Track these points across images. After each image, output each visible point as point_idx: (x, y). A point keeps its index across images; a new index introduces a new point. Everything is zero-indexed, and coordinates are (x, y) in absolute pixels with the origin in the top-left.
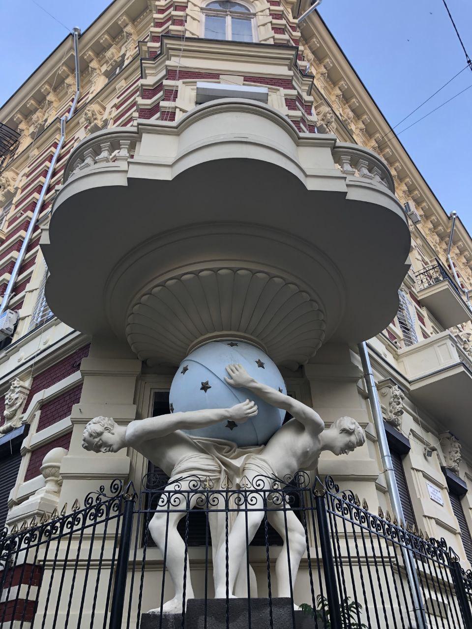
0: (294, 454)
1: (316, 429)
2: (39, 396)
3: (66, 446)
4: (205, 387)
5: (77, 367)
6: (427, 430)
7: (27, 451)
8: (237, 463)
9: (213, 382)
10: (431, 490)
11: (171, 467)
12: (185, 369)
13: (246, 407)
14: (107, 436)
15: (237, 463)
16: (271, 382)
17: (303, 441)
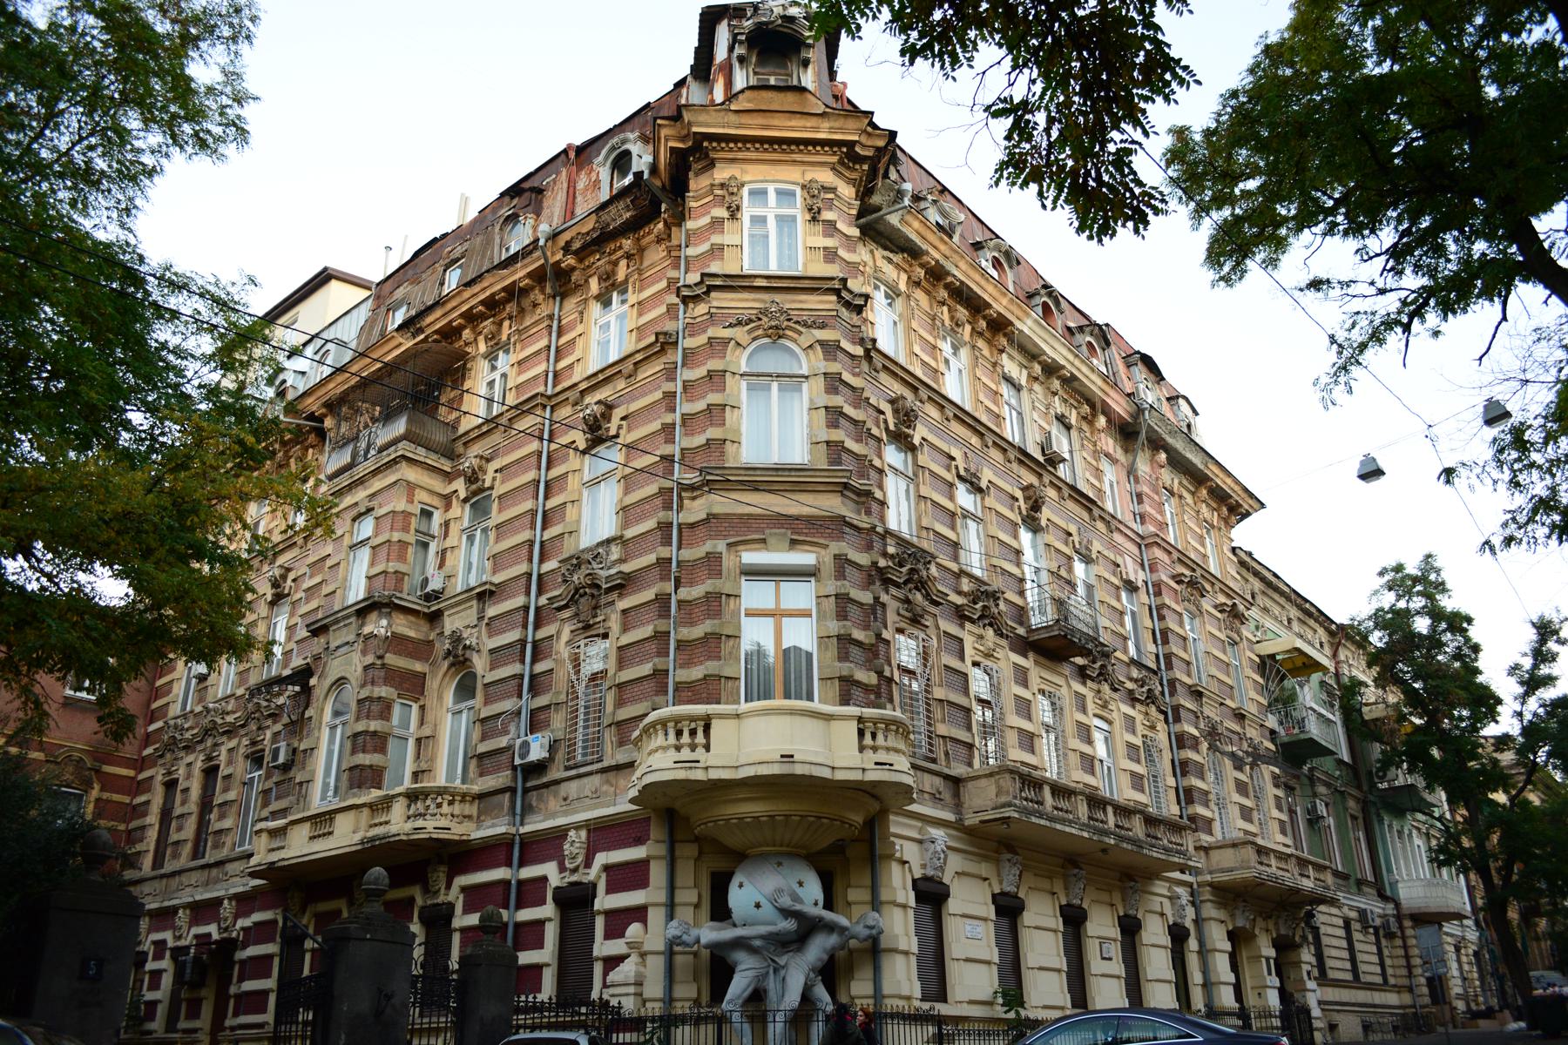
0: (825, 951)
1: (843, 930)
2: (601, 859)
3: (643, 920)
4: (758, 906)
5: (639, 841)
6: (985, 858)
7: (599, 913)
8: (782, 961)
9: (763, 901)
10: (968, 928)
11: (736, 964)
12: (741, 886)
13: (789, 925)
14: (685, 937)
15: (782, 961)
16: (811, 891)
17: (833, 940)
